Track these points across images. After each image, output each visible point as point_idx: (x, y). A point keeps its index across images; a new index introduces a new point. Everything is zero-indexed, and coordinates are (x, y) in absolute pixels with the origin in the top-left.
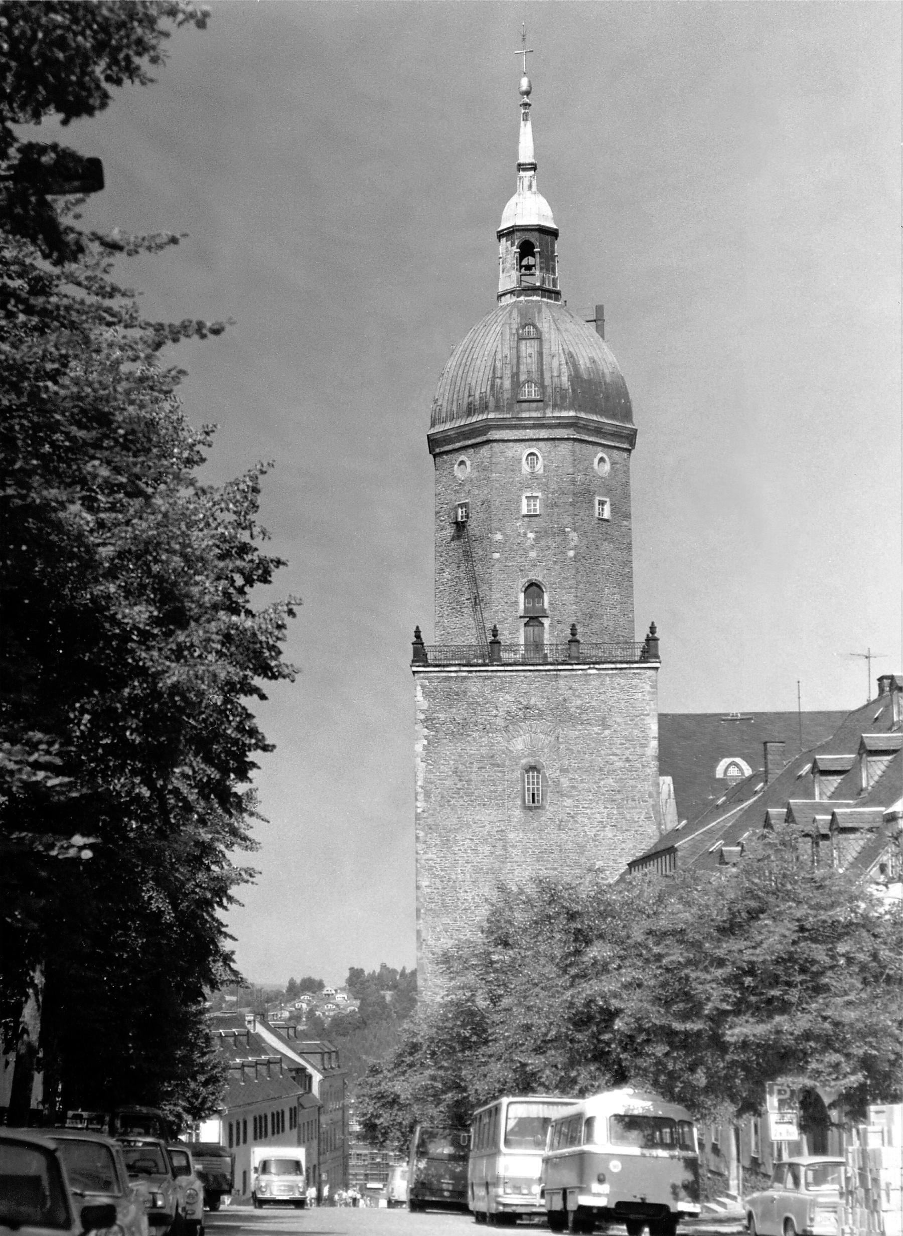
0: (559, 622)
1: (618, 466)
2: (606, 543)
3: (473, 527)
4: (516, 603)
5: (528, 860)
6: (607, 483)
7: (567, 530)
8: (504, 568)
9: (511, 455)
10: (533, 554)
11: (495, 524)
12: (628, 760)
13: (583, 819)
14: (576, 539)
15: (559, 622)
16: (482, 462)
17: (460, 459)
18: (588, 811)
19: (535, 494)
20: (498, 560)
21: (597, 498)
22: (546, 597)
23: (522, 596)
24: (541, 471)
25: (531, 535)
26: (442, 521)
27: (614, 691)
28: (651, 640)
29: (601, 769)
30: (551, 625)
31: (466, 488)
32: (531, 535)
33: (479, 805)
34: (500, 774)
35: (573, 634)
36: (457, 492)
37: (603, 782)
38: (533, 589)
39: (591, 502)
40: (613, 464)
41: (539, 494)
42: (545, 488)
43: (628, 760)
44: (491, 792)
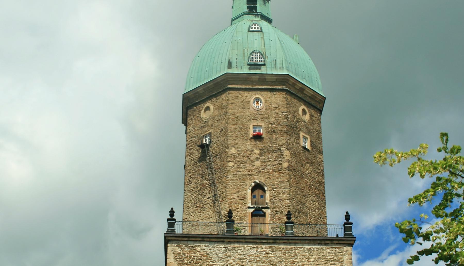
2: (308, 165)
3: (214, 149)
4: (245, 197)
6: (307, 126)
7: (282, 148)
9: (242, 99)
10: (258, 164)
11: (231, 142)
14: (288, 154)
15: (277, 212)
16: (222, 104)
19: (259, 124)
20: (232, 167)
21: (302, 134)
22: (267, 194)
23: (249, 192)
24: (264, 110)
25: (257, 151)
26: (190, 149)
27: (320, 260)
30: (272, 214)
31: (210, 124)
32: (257, 151)
35: (289, 218)
36: (203, 127)
38: (258, 187)
39: (298, 134)
40: (311, 116)
41: (263, 124)
42: (266, 120)
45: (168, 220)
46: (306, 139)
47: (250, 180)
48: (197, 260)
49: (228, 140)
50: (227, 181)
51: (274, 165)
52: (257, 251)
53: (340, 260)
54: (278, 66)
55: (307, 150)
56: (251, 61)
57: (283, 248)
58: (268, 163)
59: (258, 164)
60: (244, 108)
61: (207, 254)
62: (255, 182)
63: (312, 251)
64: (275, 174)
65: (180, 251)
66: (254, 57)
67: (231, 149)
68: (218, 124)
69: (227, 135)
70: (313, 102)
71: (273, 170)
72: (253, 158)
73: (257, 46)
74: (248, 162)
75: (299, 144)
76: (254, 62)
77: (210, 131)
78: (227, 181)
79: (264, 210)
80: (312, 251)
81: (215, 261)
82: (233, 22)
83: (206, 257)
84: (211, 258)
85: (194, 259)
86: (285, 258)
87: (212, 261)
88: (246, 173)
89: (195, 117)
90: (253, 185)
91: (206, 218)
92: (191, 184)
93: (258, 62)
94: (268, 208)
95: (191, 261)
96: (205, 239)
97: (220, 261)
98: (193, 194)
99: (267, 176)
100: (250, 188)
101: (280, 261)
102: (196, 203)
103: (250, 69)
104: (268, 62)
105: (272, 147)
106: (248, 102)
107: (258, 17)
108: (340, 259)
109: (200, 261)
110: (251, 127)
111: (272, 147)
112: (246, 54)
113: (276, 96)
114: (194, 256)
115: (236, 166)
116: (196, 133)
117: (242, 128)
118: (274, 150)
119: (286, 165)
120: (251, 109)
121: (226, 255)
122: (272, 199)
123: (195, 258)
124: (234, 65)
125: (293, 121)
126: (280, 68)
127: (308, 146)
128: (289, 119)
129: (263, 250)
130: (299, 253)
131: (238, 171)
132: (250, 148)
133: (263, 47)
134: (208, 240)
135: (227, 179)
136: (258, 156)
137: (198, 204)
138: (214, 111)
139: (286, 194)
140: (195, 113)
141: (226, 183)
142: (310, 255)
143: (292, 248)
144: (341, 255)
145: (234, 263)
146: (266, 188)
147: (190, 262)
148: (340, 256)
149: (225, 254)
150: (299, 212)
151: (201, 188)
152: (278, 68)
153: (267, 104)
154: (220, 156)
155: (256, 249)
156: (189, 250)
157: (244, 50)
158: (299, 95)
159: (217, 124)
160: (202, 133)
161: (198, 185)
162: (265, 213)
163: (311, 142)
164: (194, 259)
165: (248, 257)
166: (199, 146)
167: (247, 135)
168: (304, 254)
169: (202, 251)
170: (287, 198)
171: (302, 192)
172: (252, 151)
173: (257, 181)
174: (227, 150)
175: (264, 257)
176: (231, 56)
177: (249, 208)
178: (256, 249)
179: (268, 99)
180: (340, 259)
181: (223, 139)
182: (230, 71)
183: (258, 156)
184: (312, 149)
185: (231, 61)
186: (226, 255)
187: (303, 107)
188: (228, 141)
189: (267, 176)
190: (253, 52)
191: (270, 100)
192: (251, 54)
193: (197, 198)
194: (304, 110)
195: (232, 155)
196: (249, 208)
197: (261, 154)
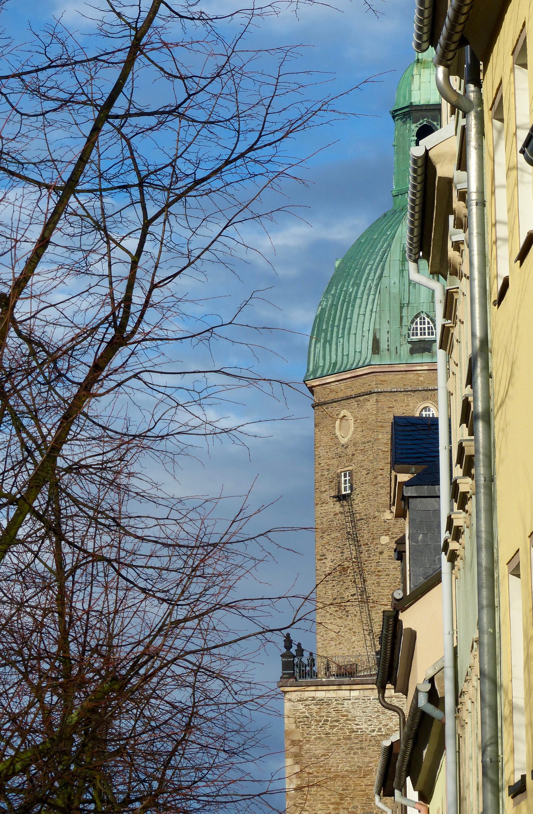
31: (349, 451)
45: (283, 656)
48: (331, 722)
49: (377, 494)
50: (379, 571)
56: (413, 335)
65: (304, 710)
66: (419, 326)
67: (385, 511)
68: (361, 456)
69: (376, 484)
76: (419, 337)
78: (379, 571)
81: (360, 723)
83: (347, 716)
84: (355, 717)
85: (328, 721)
87: (356, 722)
95: (323, 724)
97: (369, 723)
103: (412, 352)
109: (337, 724)
114: (327, 716)
121: (379, 712)
123: (329, 719)
124: (383, 345)
134: (348, 687)
135: (379, 568)
141: (377, 575)
145: (391, 724)
147: (321, 727)
149: (376, 709)
156: (318, 707)
159: (361, 457)
164: (328, 721)
174: (377, 514)
176: (377, 327)
181: (370, 490)
185: (378, 337)
186: (379, 712)
188: (379, 497)
190: (416, 317)
192: (412, 322)
193: (336, 591)
195: (385, 522)
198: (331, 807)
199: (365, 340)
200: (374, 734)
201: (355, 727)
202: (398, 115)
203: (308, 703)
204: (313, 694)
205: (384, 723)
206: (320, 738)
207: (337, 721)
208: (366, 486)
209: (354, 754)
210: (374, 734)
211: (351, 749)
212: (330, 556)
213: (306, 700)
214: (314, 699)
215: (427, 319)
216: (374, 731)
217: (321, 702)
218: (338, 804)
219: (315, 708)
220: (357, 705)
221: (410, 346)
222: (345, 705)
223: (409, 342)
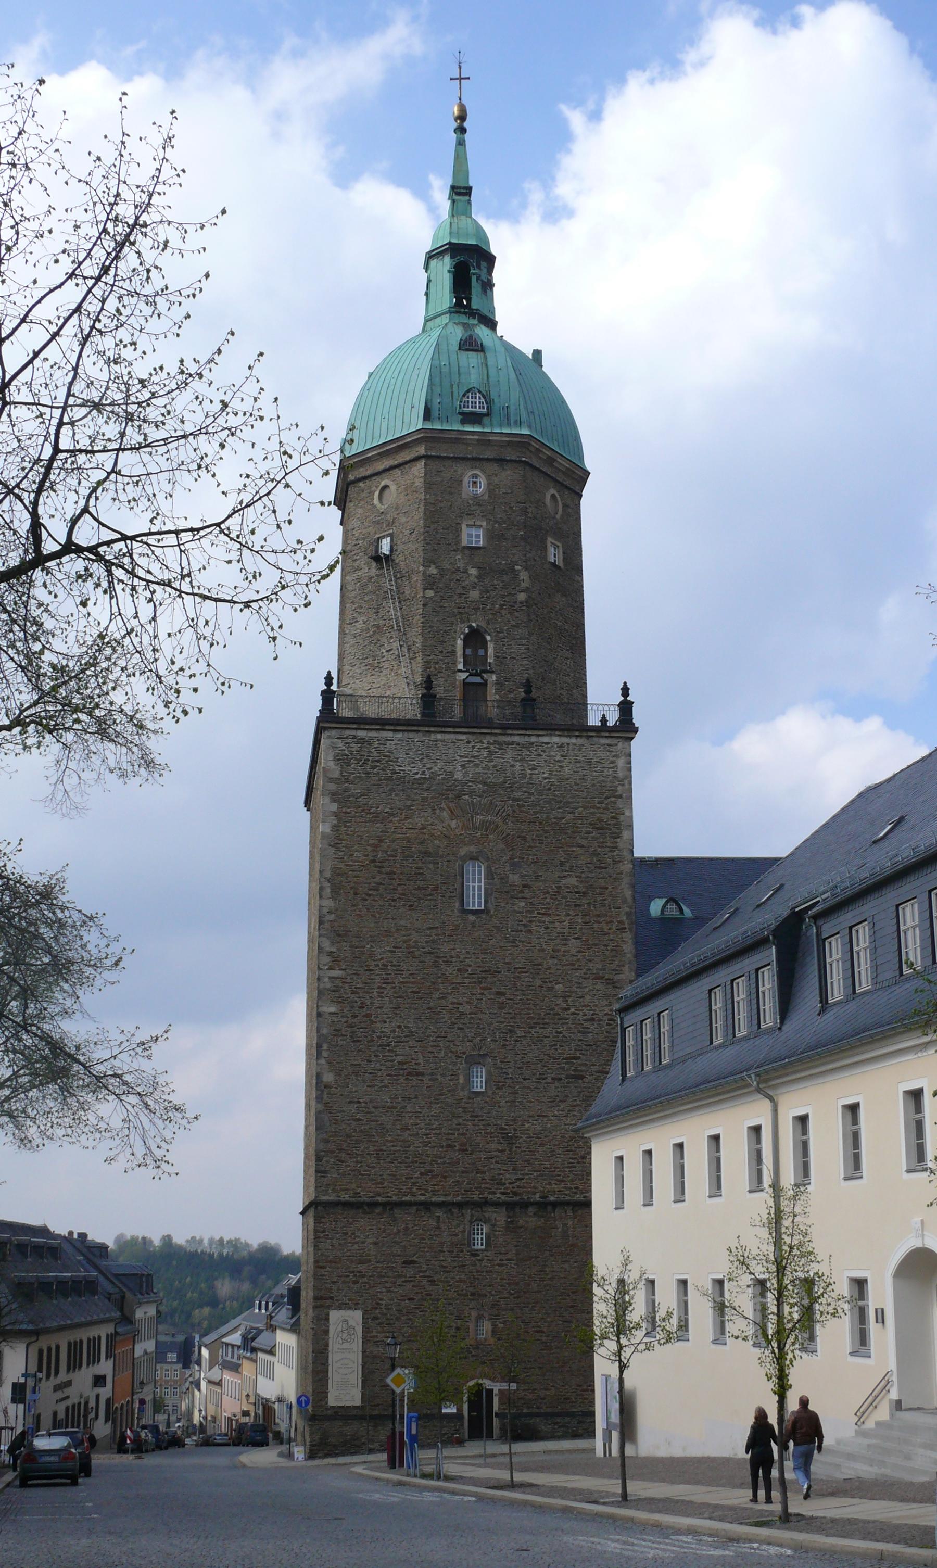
0: (507, 680)
1: (570, 510)
4: (453, 653)
5: (466, 981)
7: (517, 568)
8: (438, 609)
10: (474, 595)
12: (595, 854)
13: (538, 929)
15: (507, 680)
17: (383, 483)
18: (546, 919)
20: (431, 598)
21: (550, 539)
23: (460, 643)
24: (486, 497)
25: (473, 571)
27: (578, 765)
28: (626, 707)
29: (562, 864)
30: (497, 683)
33: (404, 906)
34: (431, 866)
35: (528, 692)
37: (564, 882)
39: (543, 541)
43: (595, 854)
44: (419, 888)
46: (556, 547)
47: (462, 622)
51: (503, 596)
52: (473, 747)
53: (611, 765)
54: (512, 419)
55: (558, 567)
57: (518, 744)
58: (493, 594)
59: (474, 595)
60: (451, 493)
61: (389, 752)
62: (470, 627)
63: (566, 749)
64: (503, 612)
66: (470, 400)
70: (567, 482)
71: (502, 606)
72: (467, 583)
73: (474, 379)
74: (458, 591)
75: (545, 557)
76: (470, 409)
77: (391, 531)
79: (485, 676)
80: (566, 749)
82: (430, 324)
83: (389, 756)
86: (521, 760)
88: (456, 610)
89: (362, 503)
90: (467, 631)
91: (384, 685)
92: (357, 624)
93: (478, 409)
94: (492, 672)
96: (387, 727)
97: (413, 765)
98: (361, 642)
99: (490, 616)
100: (462, 636)
101: (513, 766)
102: (367, 658)
103: (463, 422)
104: (496, 408)
105: (500, 563)
106: (460, 482)
107: (474, 318)
108: (613, 762)
110: (464, 526)
111: (500, 563)
112: (455, 394)
113: (508, 472)
115: (437, 599)
116: (364, 531)
117: (447, 529)
118: (504, 570)
119: (522, 597)
120: (464, 496)
122: (498, 657)
124: (435, 413)
125: (535, 518)
126: (516, 422)
127: (559, 561)
128: (530, 515)
129: (485, 746)
130: (544, 751)
131: (441, 607)
132: (461, 565)
133: (485, 382)
134: (392, 728)
136: (476, 581)
137: (370, 660)
138: (398, 494)
139: (523, 648)
140: (364, 495)
142: (562, 756)
143: (533, 743)
144: (614, 756)
146: (488, 638)
148: (611, 759)
150: (543, 679)
151: (374, 632)
152: (512, 421)
153: (491, 487)
154: (409, 578)
155: (473, 744)
157: (452, 386)
158: (549, 471)
159: (403, 519)
160: (375, 533)
161: (369, 626)
162: (486, 681)
163: (564, 553)
165: (458, 758)
166: (372, 557)
167: (458, 541)
168: (552, 753)
169: (382, 747)
170: (524, 656)
171: (549, 643)
172: (466, 571)
173: (474, 625)
175: (485, 758)
177: (460, 671)
178: (473, 744)
179: (493, 478)
180: (613, 762)
181: (414, 548)
182: (428, 426)
183: (476, 581)
184: (565, 565)
187: (552, 491)
189: (490, 616)
190: (468, 391)
191: (496, 480)
192: (464, 395)
194: (553, 496)
196: (460, 671)
197: (480, 577)
198: (369, 848)
199: (415, 410)
200: (417, 776)
201: (397, 768)
202: (434, 255)
203: (349, 741)
204: (353, 732)
205: (428, 766)
206: (360, 777)
207: (378, 761)
208: (410, 545)
209: (396, 795)
210: (417, 776)
211: (392, 790)
212: (361, 619)
213: (347, 738)
214: (355, 737)
215: (478, 395)
216: (417, 773)
217: (361, 741)
218: (376, 846)
219: (355, 747)
220: (399, 747)
221: (460, 417)
222: (388, 746)
223: (459, 413)
